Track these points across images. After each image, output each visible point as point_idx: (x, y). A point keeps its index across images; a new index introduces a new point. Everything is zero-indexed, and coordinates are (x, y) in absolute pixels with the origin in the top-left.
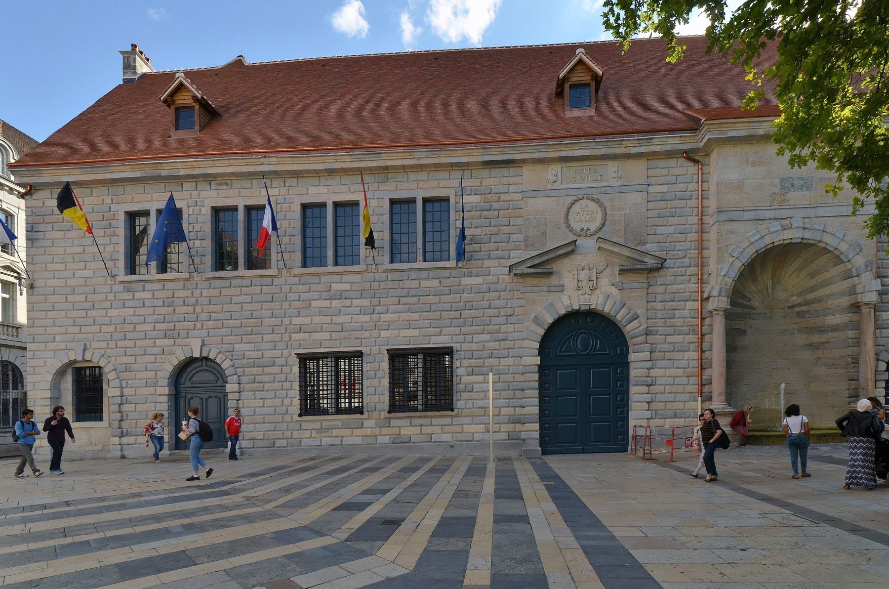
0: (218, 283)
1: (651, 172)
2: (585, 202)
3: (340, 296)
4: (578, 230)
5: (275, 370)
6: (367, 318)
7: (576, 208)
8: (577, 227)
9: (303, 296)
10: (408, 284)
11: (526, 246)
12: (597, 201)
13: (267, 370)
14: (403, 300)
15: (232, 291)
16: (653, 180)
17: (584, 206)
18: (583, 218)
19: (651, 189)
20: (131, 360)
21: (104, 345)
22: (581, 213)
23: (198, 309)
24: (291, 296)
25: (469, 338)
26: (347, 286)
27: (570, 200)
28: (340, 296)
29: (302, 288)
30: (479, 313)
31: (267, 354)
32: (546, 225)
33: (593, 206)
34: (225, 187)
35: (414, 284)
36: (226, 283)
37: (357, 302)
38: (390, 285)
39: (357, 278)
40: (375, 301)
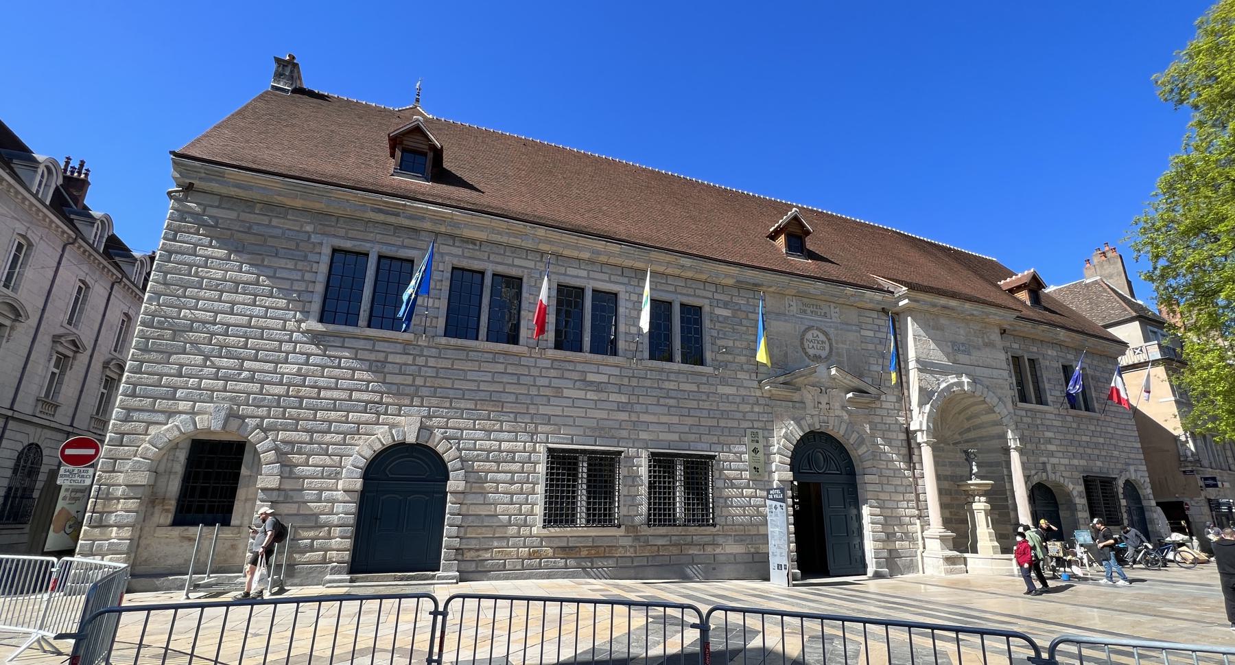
0: (450, 354)
3: (598, 387)
5: (516, 467)
6: (623, 416)
7: (809, 336)
9: (555, 383)
10: (667, 385)
12: (826, 334)
13: (503, 466)
14: (662, 401)
15: (468, 366)
18: (815, 345)
19: (864, 333)
20: (305, 437)
21: (262, 411)
23: (419, 381)
24: (541, 381)
26: (604, 379)
27: (803, 328)
28: (598, 387)
29: (553, 373)
30: (735, 424)
31: (504, 446)
33: (822, 337)
34: (471, 247)
35: (672, 386)
36: (463, 355)
37: (613, 397)
38: (648, 383)
39: (616, 371)
40: (634, 399)
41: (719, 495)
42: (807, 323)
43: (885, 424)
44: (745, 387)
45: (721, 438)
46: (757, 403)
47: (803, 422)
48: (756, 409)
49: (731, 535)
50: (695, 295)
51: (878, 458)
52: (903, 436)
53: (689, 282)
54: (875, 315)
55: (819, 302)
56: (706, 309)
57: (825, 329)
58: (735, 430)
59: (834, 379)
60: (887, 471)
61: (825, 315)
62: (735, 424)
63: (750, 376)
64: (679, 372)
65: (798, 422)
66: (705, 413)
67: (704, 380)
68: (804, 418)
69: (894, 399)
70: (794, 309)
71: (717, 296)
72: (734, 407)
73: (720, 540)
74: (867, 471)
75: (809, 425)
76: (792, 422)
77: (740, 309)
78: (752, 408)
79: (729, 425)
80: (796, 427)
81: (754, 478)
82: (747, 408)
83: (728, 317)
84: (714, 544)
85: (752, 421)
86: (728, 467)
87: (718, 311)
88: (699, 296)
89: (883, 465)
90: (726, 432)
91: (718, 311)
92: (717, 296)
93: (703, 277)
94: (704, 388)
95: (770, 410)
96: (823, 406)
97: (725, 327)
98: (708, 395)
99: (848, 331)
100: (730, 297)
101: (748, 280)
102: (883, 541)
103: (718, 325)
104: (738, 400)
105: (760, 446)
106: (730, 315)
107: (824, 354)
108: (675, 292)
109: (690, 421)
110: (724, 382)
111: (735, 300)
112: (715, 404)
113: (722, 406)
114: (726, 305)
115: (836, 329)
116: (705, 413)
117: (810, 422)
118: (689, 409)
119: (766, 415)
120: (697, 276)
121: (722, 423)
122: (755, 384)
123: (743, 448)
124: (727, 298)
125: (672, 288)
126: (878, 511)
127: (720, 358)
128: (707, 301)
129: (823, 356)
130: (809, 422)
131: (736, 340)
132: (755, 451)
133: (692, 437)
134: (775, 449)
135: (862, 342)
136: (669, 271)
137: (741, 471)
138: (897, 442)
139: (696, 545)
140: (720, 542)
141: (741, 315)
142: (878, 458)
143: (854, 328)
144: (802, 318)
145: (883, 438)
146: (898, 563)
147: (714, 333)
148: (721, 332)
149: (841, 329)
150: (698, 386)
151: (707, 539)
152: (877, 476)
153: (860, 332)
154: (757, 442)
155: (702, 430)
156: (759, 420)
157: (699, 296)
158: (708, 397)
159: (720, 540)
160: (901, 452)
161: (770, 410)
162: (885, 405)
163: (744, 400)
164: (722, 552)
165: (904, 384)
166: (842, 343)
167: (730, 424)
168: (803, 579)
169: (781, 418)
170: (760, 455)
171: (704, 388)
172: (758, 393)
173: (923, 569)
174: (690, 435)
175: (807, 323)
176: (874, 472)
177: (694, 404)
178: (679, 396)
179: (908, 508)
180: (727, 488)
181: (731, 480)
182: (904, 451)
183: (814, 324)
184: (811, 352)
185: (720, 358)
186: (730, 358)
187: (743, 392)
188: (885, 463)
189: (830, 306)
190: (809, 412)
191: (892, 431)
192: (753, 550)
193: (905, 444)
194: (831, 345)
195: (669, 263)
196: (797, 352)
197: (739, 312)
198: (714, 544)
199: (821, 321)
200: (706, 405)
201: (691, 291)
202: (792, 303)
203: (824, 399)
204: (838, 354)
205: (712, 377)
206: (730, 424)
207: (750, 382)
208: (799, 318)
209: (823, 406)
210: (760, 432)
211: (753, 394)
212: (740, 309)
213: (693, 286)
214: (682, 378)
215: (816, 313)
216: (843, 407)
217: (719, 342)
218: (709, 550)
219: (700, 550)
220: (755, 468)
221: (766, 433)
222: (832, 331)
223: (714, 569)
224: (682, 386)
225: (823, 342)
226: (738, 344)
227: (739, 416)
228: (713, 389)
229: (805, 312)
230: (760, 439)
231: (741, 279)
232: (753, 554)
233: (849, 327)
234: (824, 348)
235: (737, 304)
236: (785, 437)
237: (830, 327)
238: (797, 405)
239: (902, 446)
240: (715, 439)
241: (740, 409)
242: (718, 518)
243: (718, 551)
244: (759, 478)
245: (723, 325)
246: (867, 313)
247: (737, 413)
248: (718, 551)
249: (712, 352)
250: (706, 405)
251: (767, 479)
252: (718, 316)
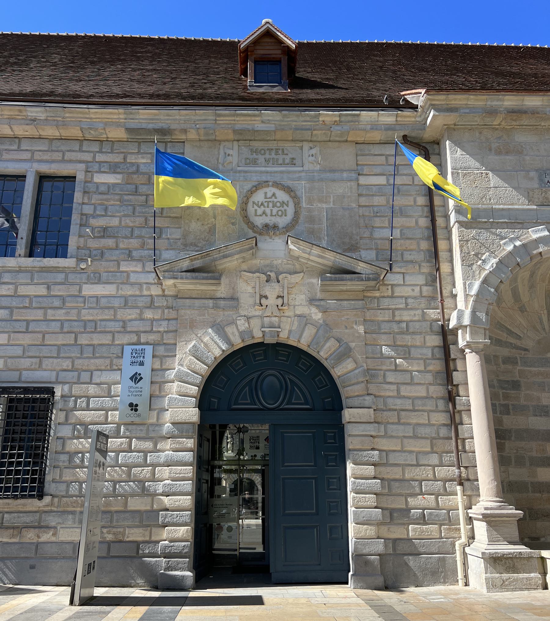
1: (362, 160)
2: (270, 191)
4: (260, 226)
7: (259, 197)
8: (259, 221)
11: (185, 245)
12: (288, 190)
16: (366, 170)
17: (269, 195)
18: (268, 211)
19: (363, 180)
22: (266, 204)
25: (85, 376)
30: (106, 339)
32: (215, 217)
33: (282, 196)
41: (59, 448)
42: (255, 179)
43: (400, 322)
44: (132, 284)
45: (78, 362)
46: (151, 305)
47: (230, 330)
48: (149, 314)
49: (73, 513)
50: (63, 161)
51: (381, 379)
52: (435, 340)
53: (56, 144)
54: (390, 149)
55: (281, 144)
56: (80, 177)
57: (290, 183)
58: (104, 349)
59: (298, 258)
60: (399, 402)
61: (292, 162)
62: (106, 339)
63: (144, 266)
64: (20, 270)
65: (220, 329)
66: (55, 326)
67: (60, 277)
68: (233, 322)
69: (421, 280)
70: (234, 159)
71: (100, 157)
72: (108, 315)
73: (52, 520)
74: (350, 402)
75: (241, 334)
76: (210, 330)
77: (137, 172)
78: (141, 313)
79: (95, 342)
80: (216, 338)
81: (129, 420)
82: (131, 314)
83: (115, 185)
84: (41, 527)
85: (138, 333)
86: (84, 405)
87: (99, 178)
88: (70, 161)
89: (389, 391)
90: (88, 352)
91: (99, 178)
92: (100, 157)
93: (76, 132)
94: (57, 291)
95: (173, 314)
96: (272, 301)
97: (107, 200)
98: (63, 299)
99: (334, 180)
100: (122, 156)
101: (144, 126)
102: (379, 524)
103: (95, 199)
104: (116, 303)
105: (145, 371)
106: (119, 181)
107: (282, 222)
108: (31, 160)
109: (26, 339)
110: (98, 280)
111: (131, 159)
112: (75, 311)
113: (86, 315)
114: (114, 168)
115: (311, 180)
116: (55, 326)
117: (242, 324)
118: (28, 322)
119: (165, 323)
120: (65, 133)
121: (83, 340)
122: (152, 278)
123: (116, 376)
124: (117, 158)
125: (26, 156)
126: (370, 470)
127: (93, 244)
128: (82, 166)
129: (281, 226)
130: (242, 328)
131: (125, 216)
132: (136, 378)
133: (26, 363)
134: (171, 374)
135: (360, 195)
136: (19, 130)
137: (107, 411)
138: (425, 351)
139: (7, 528)
140: (53, 524)
141: (138, 179)
142: (381, 379)
143: (345, 175)
144: (246, 172)
145: (393, 346)
146: (411, 564)
147: (88, 210)
148: (99, 208)
149: (321, 180)
150: (48, 288)
151: (27, 519)
152: (372, 410)
153: (357, 180)
154: (142, 364)
155: (45, 351)
156: (151, 331)
157: (70, 161)
158: (64, 303)
159: (52, 520)
160: (431, 368)
161: (173, 314)
162: (398, 291)
163: (126, 303)
164: (54, 539)
165: (443, 255)
166: (321, 201)
167: (97, 339)
168: (199, 584)
169: (192, 325)
170: (145, 384)
171: (57, 291)
172: (155, 291)
173: (466, 576)
174: (22, 360)
175: (255, 178)
176: (367, 404)
177: (39, 314)
178: (14, 304)
179: (441, 465)
180: (78, 438)
181: (85, 425)
182: (437, 366)
183: (269, 178)
184: (259, 221)
185: (93, 244)
186: (110, 242)
187: (128, 291)
188: (394, 387)
189: (301, 148)
190: (243, 313)
191: (414, 333)
192: (110, 537)
193: (439, 354)
194: (297, 204)
195: (11, 118)
196: (233, 224)
197: (135, 176)
198: (40, 527)
199: (282, 172)
200: (60, 314)
201: (58, 156)
202: (231, 152)
203: (272, 291)
204: (311, 220)
205: (73, 272)
206: (97, 339)
207: (143, 275)
208: (240, 172)
209: (272, 301)
210: (149, 350)
211: (145, 293)
212: (137, 172)
213: (63, 148)
214: (23, 278)
215: (275, 162)
216: (312, 301)
217: (93, 222)
218: (30, 536)
219: (13, 536)
220: (131, 405)
221: (161, 350)
222: (302, 187)
223: (32, 567)
224: (23, 290)
225: (283, 203)
226: (128, 221)
227: (115, 326)
228: (74, 290)
229: (254, 162)
230: (148, 359)
231: (133, 126)
232: (109, 543)
233: (337, 175)
234: (285, 213)
235: (132, 164)
236: (196, 354)
237: (299, 179)
238: (222, 303)
239: (433, 358)
240: (66, 364)
241: (119, 317)
242: (53, 485)
243: (46, 537)
244: (137, 420)
245: (105, 197)
246: (376, 150)
247: (112, 323)
248: (46, 537)
249: (80, 236)
250: (60, 314)
251: (153, 420)
252: (98, 185)
